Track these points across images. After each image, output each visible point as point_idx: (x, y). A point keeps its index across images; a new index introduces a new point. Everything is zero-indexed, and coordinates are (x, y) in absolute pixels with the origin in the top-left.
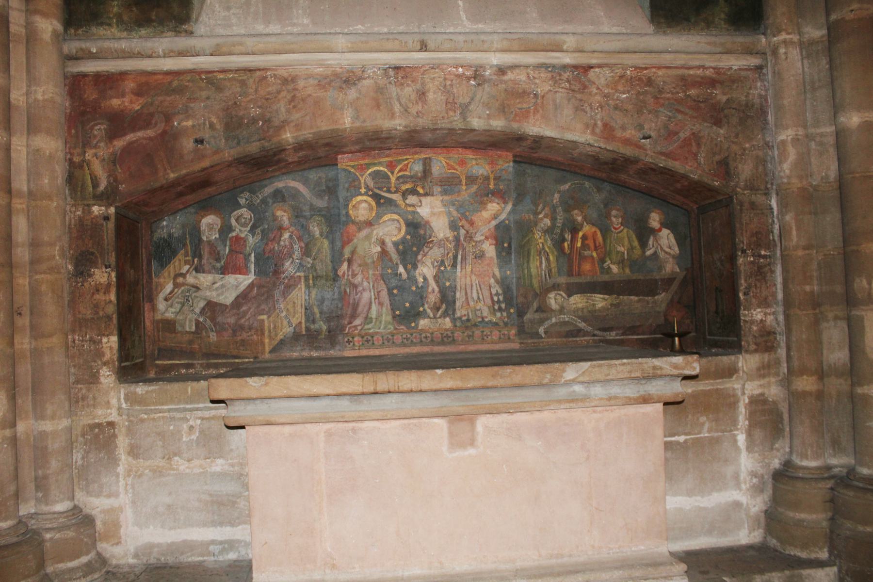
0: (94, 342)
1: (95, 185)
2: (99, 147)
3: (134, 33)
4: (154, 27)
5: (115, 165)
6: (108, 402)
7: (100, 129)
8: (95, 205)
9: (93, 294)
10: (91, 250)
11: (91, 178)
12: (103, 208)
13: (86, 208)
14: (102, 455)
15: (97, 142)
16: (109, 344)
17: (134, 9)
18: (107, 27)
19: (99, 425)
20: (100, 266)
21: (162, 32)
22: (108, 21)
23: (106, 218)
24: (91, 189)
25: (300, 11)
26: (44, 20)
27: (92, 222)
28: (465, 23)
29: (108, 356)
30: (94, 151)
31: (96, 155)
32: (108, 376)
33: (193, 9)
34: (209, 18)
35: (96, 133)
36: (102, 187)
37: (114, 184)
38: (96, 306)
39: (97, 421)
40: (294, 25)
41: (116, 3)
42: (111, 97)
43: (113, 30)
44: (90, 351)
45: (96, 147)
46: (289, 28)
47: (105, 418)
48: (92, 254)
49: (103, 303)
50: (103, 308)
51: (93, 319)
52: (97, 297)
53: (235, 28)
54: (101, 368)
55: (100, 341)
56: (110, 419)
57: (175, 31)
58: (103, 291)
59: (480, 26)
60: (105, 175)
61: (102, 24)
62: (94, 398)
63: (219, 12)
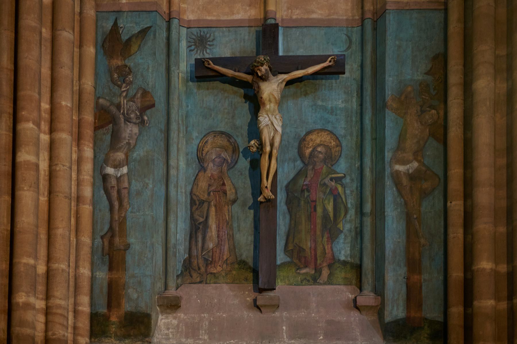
3: (122, 342)
4: (132, 339)
17: (123, 329)
21: (136, 342)
22: (110, 335)
25: (203, 332)
26: (82, 338)
28: (285, 340)
33: (151, 330)
34: (159, 335)
40: (200, 339)
41: (114, 326)
46: (198, 341)
53: (171, 340)
57: (142, 341)
59: (293, 341)
61: (107, 337)
63: (164, 331)
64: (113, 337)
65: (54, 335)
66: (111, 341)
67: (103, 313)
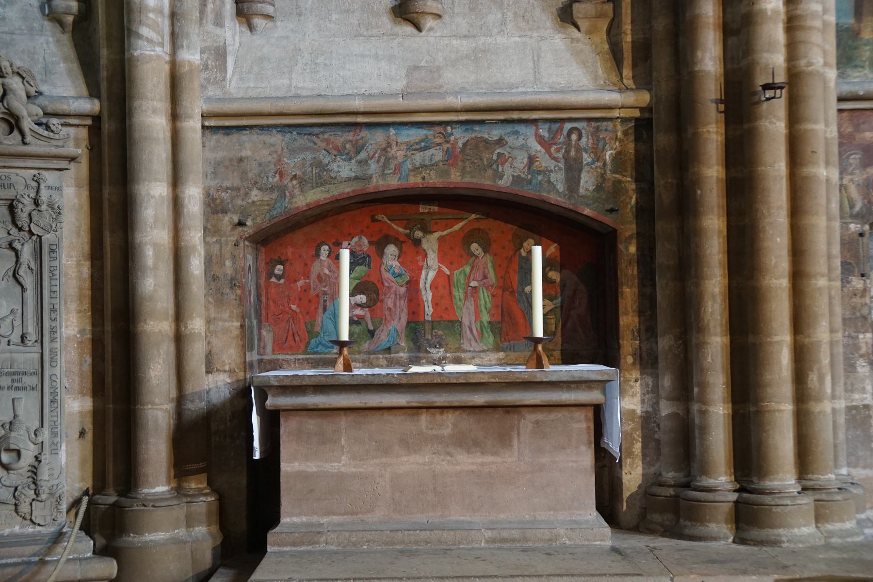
0: (852, 337)
1: (852, 207)
2: (855, 174)
5: (868, 189)
6: (864, 389)
7: (855, 158)
8: (851, 223)
9: (851, 298)
10: (849, 261)
11: (848, 200)
12: (859, 226)
13: (844, 225)
14: (858, 433)
15: (853, 169)
16: (864, 340)
18: (860, 69)
19: (856, 408)
20: (856, 274)
23: (861, 235)
24: (848, 209)
27: (849, 237)
29: (863, 350)
30: (850, 177)
31: (851, 180)
32: (864, 366)
35: (851, 161)
36: (858, 208)
37: (868, 205)
38: (854, 308)
39: (854, 404)
42: (864, 131)
43: (866, 72)
44: (849, 345)
45: (852, 174)
47: (862, 401)
48: (850, 264)
49: (859, 305)
50: (860, 310)
51: (850, 318)
52: (854, 300)
54: (858, 360)
55: (857, 337)
56: (866, 402)
58: (859, 295)
60: (861, 198)
61: (856, 67)
62: (852, 384)
64: (867, 68)
65: (810, 66)
66: (865, 74)
67: (847, 26)
